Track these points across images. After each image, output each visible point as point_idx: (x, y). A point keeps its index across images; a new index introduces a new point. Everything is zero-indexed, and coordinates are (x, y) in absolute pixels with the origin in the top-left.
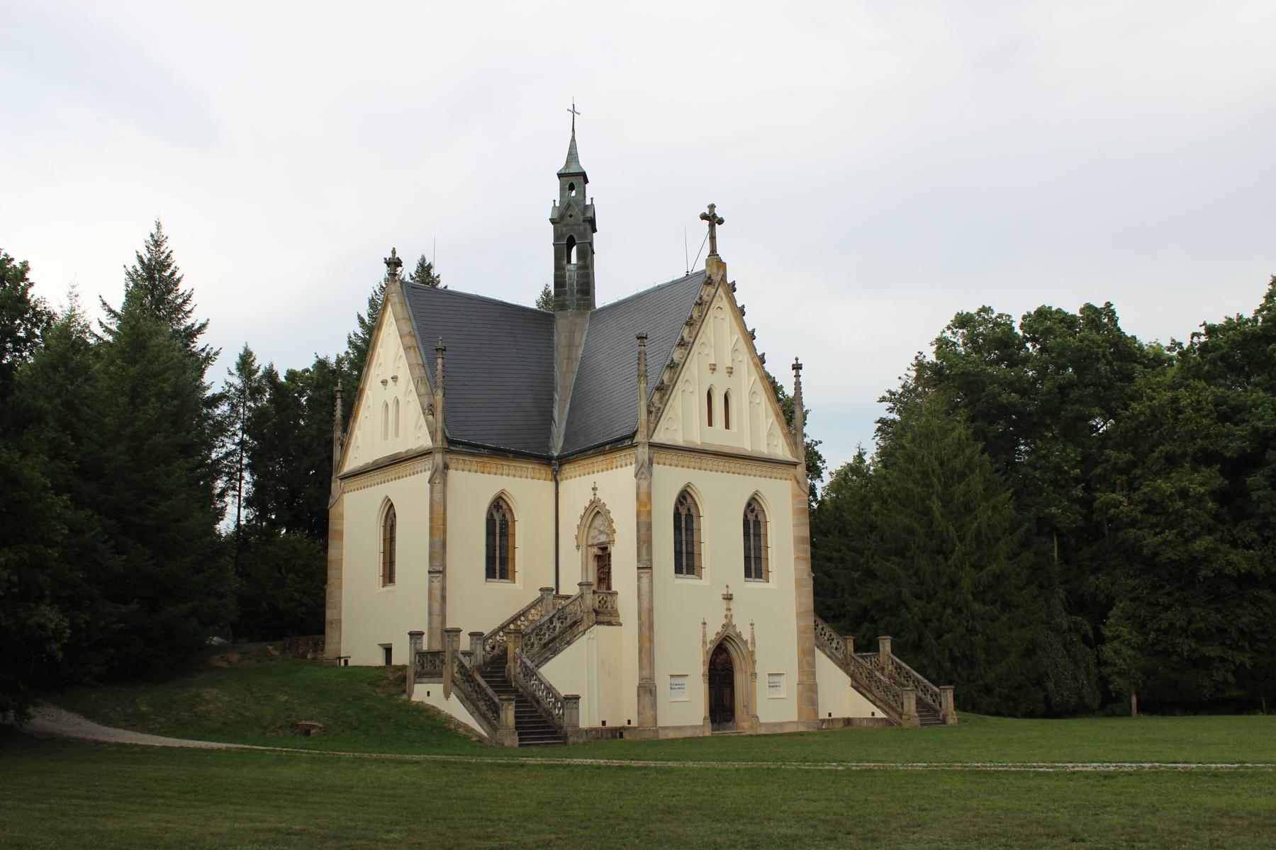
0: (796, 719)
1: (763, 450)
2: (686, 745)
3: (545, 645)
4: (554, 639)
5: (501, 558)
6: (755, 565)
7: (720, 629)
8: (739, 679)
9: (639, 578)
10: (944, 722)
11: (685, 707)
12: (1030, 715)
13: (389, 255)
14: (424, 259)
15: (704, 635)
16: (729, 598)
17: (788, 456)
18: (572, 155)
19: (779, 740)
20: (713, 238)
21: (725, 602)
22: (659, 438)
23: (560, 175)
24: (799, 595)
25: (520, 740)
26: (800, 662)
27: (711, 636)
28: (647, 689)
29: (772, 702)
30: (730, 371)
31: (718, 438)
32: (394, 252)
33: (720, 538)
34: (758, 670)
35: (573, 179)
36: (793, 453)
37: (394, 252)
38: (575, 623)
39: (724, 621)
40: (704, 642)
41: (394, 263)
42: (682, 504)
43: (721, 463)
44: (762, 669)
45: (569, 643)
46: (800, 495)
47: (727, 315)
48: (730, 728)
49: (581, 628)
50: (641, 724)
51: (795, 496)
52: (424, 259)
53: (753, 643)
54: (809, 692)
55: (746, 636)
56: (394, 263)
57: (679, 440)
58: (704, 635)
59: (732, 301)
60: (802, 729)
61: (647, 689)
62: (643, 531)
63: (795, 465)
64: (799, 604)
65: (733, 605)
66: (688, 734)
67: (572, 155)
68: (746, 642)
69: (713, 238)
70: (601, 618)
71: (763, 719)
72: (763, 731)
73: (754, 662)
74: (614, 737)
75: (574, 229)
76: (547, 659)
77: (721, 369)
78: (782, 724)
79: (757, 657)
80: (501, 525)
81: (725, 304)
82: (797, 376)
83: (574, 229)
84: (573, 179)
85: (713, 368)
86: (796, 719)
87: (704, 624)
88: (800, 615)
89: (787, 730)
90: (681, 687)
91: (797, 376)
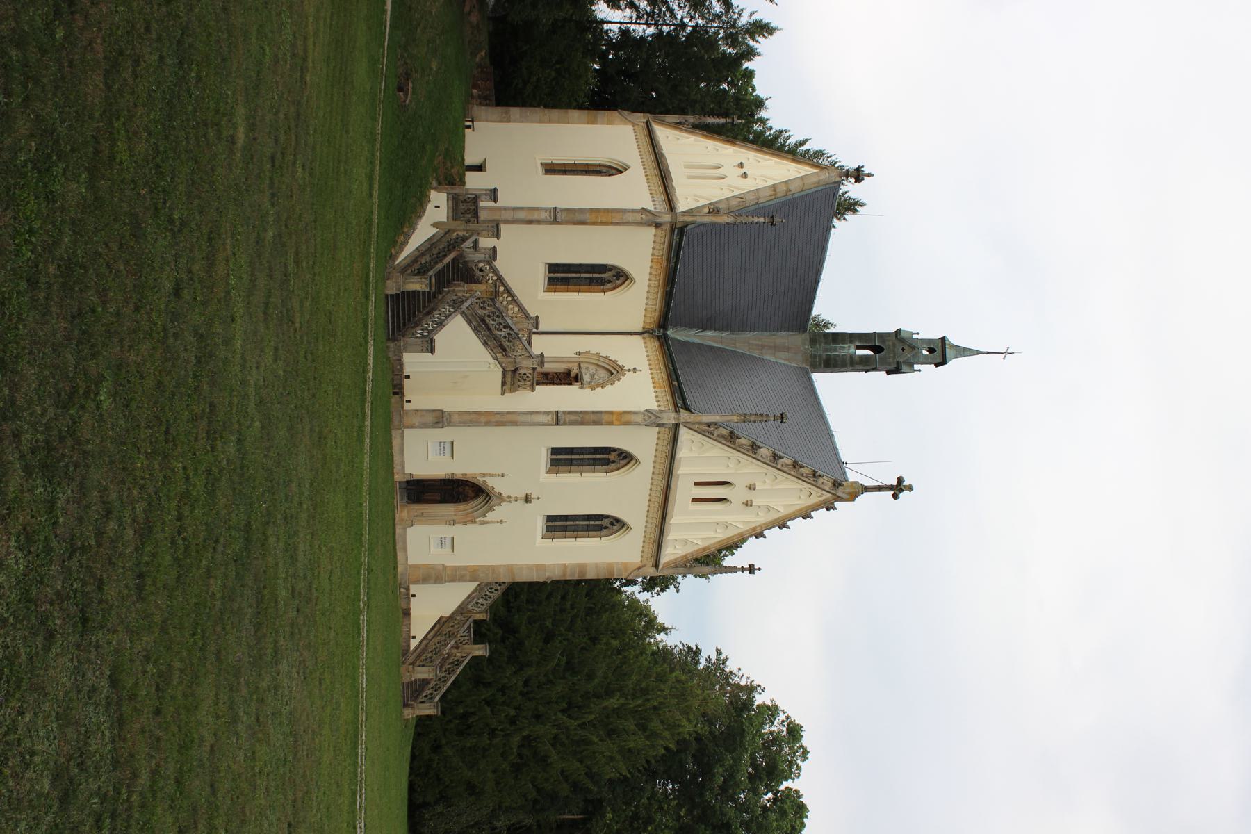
0: (410, 562)
1: (671, 535)
2: (386, 456)
3: (483, 320)
4: (488, 328)
5: (568, 279)
6: (559, 525)
7: (497, 490)
8: (449, 509)
9: (548, 413)
10: (406, 705)
11: (422, 456)
12: (412, 788)
13: (866, 170)
14: (862, 205)
15: (491, 475)
16: (527, 499)
17: (664, 560)
18: (963, 352)
19: (390, 546)
20: (879, 488)
21: (522, 495)
22: (684, 433)
23: (943, 339)
24: (530, 568)
25: (392, 296)
26: (465, 568)
27: (491, 482)
28: (440, 419)
29: (426, 540)
30: (748, 504)
31: (683, 490)
32: (869, 175)
33: (586, 492)
35: (940, 352)
36: (667, 565)
37: (869, 175)
38: (505, 350)
39: (505, 495)
40: (485, 475)
41: (858, 175)
42: (619, 455)
43: (659, 494)
44: (458, 531)
45: (485, 344)
46: (626, 570)
47: (803, 502)
49: (499, 356)
50: (407, 412)
51: (625, 565)
52: (862, 205)
53: (484, 523)
54: (436, 576)
55: (490, 516)
56: (858, 175)
57: (682, 453)
58: (491, 475)
59: (817, 507)
60: (400, 568)
61: (440, 419)
62: (593, 417)
63: (656, 565)
64: (521, 568)
65: (521, 503)
66: (397, 458)
67: (963, 352)
69: (879, 488)
70: (509, 375)
71: (411, 532)
72: (399, 530)
73: (465, 523)
74: (394, 386)
75: (891, 353)
76: (469, 322)
77: (749, 495)
78: (405, 549)
79: (470, 526)
80: (601, 279)
81: (815, 499)
82: (743, 569)
83: (891, 353)
84: (940, 352)
85: (751, 487)
86: (410, 562)
88: (510, 568)
90: (442, 452)
91: (743, 569)
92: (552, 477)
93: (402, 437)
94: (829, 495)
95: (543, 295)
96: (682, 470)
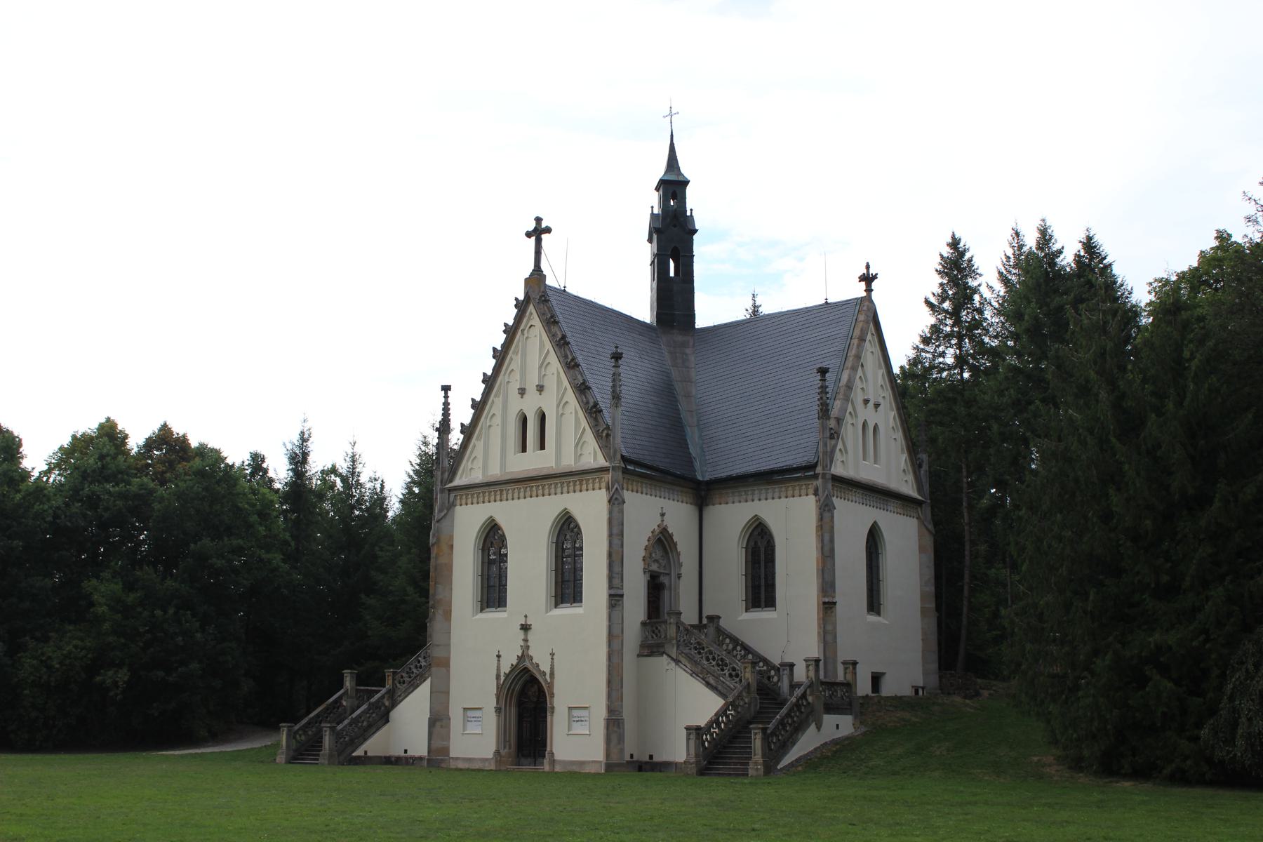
6: (567, 588)
27: (506, 668)
31: (534, 462)
33: (529, 567)
35: (673, 187)
40: (498, 677)
53: (552, 674)
55: (545, 667)
61: (438, 721)
65: (531, 636)
66: (476, 766)
68: (544, 674)
72: (558, 768)
75: (673, 234)
78: (582, 763)
82: (446, 397)
83: (673, 234)
84: (673, 187)
87: (499, 656)
89: (587, 769)
90: (478, 719)
91: (446, 397)
93: (457, 759)
94: (531, 308)
95: (746, 616)
96: (495, 472)
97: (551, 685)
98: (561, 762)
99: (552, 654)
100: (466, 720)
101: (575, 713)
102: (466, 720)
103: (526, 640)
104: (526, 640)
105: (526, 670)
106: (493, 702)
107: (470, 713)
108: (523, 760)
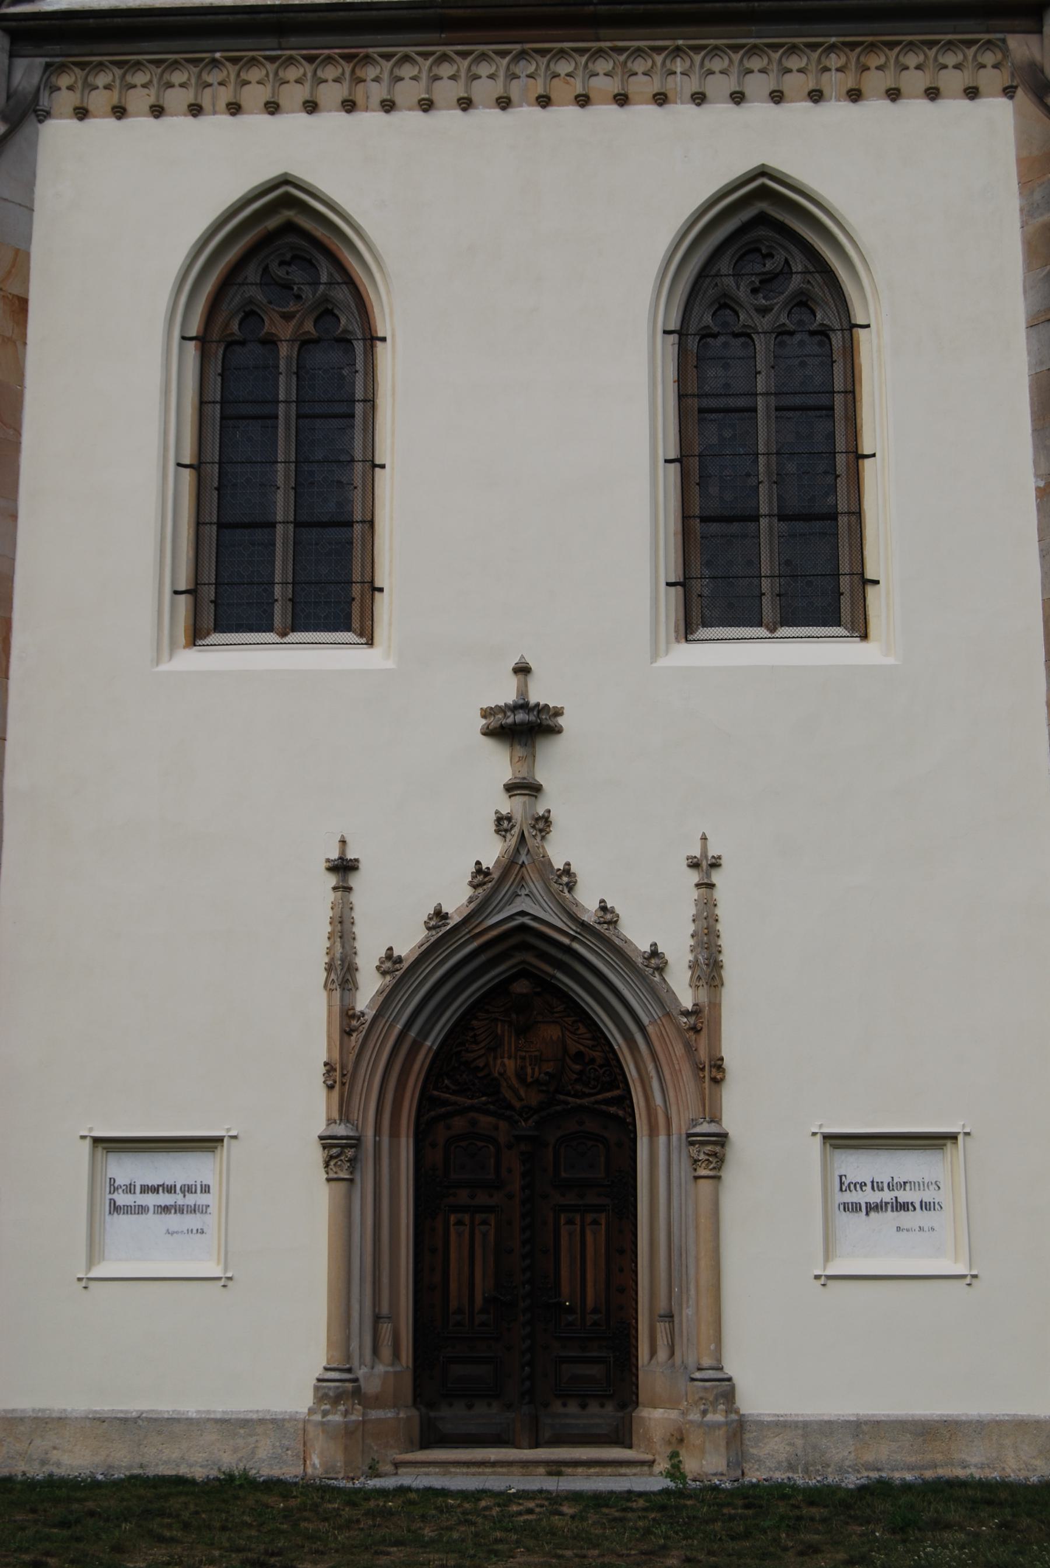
7: (457, 900)
15: (342, 928)
16: (524, 727)
21: (499, 764)
27: (394, 924)
34: (735, 1116)
39: (492, 852)
40: (342, 973)
48: (622, 1436)
53: (709, 969)
55: (655, 922)
58: (342, 928)
65: (553, 765)
71: (758, 1398)
72: (768, 1463)
73: (713, 1072)
79: (734, 1046)
90: (177, 1202)
92: (385, 608)
97: (702, 1023)
98: (782, 1426)
99: (705, 866)
100: (109, 1204)
101: (859, 1166)
102: (109, 1204)
103: (525, 788)
104: (525, 788)
105: (523, 937)
106: (312, 1111)
107: (126, 1169)
108: (452, 1416)
